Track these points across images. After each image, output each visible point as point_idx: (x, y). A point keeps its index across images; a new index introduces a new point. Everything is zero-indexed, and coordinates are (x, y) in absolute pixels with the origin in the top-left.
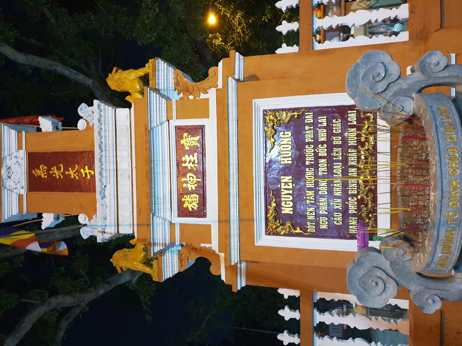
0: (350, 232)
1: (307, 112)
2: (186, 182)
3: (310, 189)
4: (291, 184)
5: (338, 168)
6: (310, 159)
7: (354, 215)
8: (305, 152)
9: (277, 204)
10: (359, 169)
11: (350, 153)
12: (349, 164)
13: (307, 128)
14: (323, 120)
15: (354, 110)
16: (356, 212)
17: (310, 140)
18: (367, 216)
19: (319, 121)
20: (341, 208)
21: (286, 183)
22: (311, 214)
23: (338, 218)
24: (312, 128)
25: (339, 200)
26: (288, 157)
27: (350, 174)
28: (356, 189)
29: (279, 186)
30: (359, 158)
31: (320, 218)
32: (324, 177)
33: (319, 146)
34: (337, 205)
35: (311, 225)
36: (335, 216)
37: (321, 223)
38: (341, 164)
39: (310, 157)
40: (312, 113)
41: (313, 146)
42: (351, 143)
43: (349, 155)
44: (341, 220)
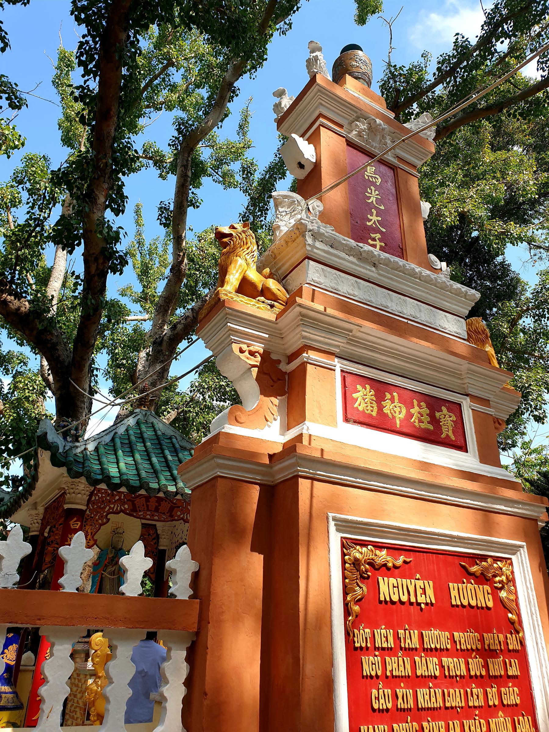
2: (392, 400)
29: (418, 576)
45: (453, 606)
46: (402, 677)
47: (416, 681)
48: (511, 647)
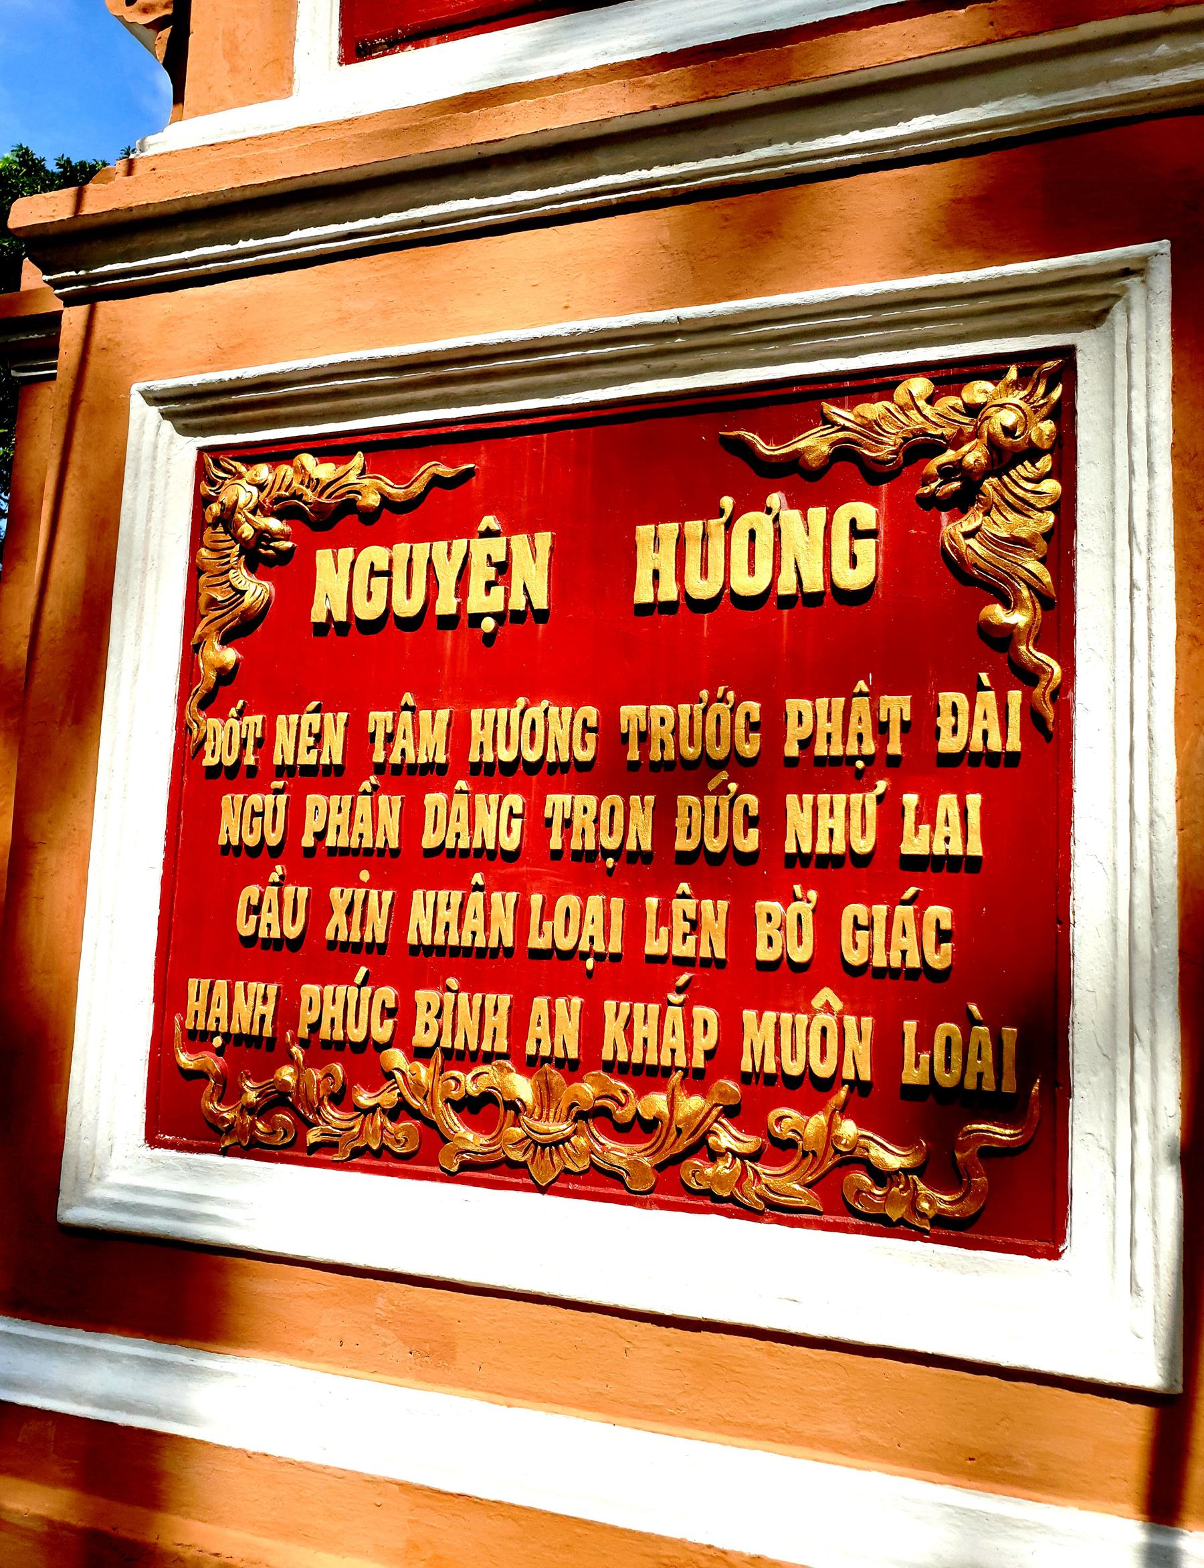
0: (193, 983)
1: (1026, 698)
3: (459, 733)
4: (495, 601)
5: (586, 923)
6: (660, 732)
7: (287, 1011)
8: (713, 699)
10: (572, 1069)
12: (609, 1006)
13: (897, 707)
14: (951, 827)
15: (1024, 1082)
16: (303, 1032)
17: (795, 733)
18: (277, 1099)
19: (947, 803)
20: (330, 934)
21: (503, 569)
23: (271, 910)
24: (895, 748)
25: (378, 930)
26: (680, 576)
27: (540, 1004)
28: (446, 1042)
30: (648, 1076)
31: (282, 798)
32: (536, 824)
33: (752, 800)
34: (349, 911)
35: (244, 743)
37: (256, 799)
38: (616, 946)
39: (675, 731)
40: (1014, 744)
41: (750, 749)
43: (675, 1015)
44: (263, 933)
45: (644, 609)
46: (356, 852)
47: (410, 866)
48: (948, 744)
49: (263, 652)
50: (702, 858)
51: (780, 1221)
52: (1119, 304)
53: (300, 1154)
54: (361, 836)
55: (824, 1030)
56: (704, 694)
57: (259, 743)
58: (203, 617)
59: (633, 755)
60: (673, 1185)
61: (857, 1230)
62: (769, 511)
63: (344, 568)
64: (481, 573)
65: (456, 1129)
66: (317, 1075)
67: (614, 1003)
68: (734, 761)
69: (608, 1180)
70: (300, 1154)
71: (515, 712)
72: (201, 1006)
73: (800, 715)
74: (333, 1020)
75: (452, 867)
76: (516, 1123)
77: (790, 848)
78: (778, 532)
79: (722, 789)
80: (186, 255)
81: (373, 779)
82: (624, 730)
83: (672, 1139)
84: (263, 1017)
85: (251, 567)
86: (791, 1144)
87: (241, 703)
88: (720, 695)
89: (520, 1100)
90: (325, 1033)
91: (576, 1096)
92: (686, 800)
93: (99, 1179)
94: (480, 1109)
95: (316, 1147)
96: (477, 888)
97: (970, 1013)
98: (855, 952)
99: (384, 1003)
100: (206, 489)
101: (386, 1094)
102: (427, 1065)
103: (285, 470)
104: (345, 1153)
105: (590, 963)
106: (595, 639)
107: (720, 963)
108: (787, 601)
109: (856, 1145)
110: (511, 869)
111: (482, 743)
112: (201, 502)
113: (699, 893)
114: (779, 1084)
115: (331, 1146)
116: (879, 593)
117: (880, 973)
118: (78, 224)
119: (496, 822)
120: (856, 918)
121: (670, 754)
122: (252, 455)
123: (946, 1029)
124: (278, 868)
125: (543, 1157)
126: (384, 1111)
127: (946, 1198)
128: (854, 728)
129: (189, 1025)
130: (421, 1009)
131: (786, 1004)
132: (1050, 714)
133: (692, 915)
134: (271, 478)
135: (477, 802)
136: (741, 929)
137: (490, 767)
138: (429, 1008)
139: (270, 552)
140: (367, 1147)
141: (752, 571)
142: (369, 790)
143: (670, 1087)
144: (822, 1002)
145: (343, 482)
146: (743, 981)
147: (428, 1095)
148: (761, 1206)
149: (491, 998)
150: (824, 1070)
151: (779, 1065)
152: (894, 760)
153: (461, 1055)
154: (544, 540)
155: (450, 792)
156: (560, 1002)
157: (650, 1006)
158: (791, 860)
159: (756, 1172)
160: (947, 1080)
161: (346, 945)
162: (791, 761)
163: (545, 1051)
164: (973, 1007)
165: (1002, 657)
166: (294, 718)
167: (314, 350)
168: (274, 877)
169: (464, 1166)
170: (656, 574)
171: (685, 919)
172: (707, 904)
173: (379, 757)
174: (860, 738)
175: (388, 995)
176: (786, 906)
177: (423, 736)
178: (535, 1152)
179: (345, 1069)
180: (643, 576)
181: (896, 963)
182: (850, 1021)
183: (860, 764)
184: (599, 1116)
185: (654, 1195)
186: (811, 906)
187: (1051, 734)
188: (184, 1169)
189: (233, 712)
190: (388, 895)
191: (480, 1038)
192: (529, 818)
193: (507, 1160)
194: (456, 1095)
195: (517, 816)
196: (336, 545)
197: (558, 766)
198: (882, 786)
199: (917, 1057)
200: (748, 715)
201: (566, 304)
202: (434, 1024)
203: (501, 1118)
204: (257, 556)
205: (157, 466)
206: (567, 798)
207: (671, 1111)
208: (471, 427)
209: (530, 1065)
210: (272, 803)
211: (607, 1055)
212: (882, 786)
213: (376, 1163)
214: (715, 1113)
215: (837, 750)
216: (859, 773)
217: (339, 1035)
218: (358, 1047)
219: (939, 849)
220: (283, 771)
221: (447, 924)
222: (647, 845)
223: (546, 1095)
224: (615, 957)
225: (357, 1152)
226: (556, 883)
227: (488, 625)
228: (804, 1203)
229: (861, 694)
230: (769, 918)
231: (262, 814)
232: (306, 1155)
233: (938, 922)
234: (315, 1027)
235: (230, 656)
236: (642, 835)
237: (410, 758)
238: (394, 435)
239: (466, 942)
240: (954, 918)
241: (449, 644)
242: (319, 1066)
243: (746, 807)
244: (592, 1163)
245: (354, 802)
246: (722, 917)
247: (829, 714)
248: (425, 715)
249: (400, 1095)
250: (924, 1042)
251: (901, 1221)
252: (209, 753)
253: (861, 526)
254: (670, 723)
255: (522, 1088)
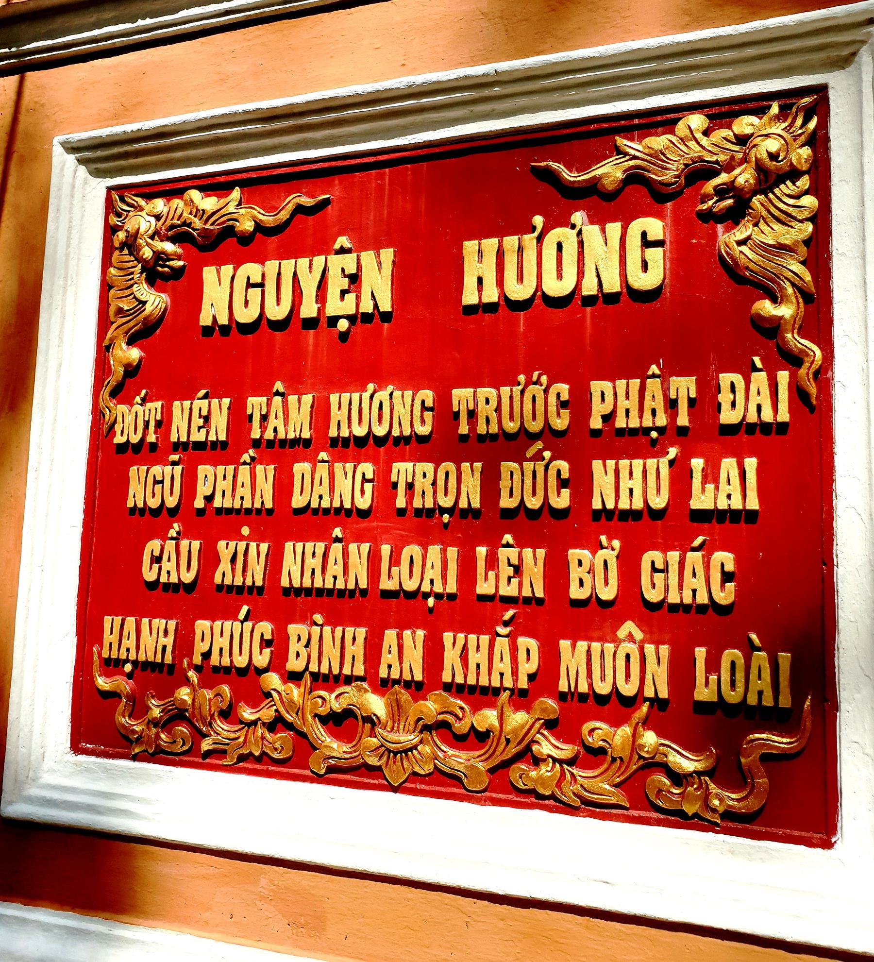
0: (108, 620)
3: (320, 414)
4: (348, 306)
5: (427, 568)
6: (484, 410)
7: (184, 642)
9: (252, 234)
10: (417, 689)
11: (514, 649)
12: (448, 637)
13: (684, 386)
14: (732, 486)
16: (197, 660)
17: (599, 409)
18: (177, 715)
19: (729, 465)
20: (218, 579)
21: (355, 279)
22: (198, 422)
23: (170, 560)
24: (683, 420)
25: (257, 575)
26: (500, 282)
27: (390, 635)
28: (313, 668)
29: (343, 241)
30: (481, 695)
31: (178, 469)
32: (385, 487)
33: (563, 466)
34: (233, 560)
35: (147, 424)
36: (184, 543)
37: (157, 470)
38: (452, 587)
39: (498, 409)
40: (784, 415)
41: (561, 423)
42: (573, 656)
43: (502, 644)
45: (471, 310)
46: (238, 511)
47: (282, 522)
48: (728, 417)
49: (163, 351)
50: (522, 513)
51: (593, 815)
52: (865, 47)
53: (196, 760)
54: (242, 498)
55: (628, 656)
56: (522, 378)
57: (158, 424)
58: (113, 323)
59: (464, 429)
60: (504, 785)
61: (658, 823)
62: (573, 227)
63: (226, 282)
64: (337, 283)
65: (323, 739)
66: (209, 694)
67: (452, 634)
68: (548, 433)
69: (449, 781)
70: (196, 760)
71: (366, 396)
72: (114, 638)
73: (603, 394)
74: (221, 649)
75: (316, 522)
76: (373, 734)
77: (597, 504)
78: (581, 244)
79: (538, 457)
80: (96, 32)
81: (251, 452)
82: (455, 409)
83: (501, 747)
84: (164, 648)
85: (151, 282)
86: (602, 751)
87: (144, 392)
88: (535, 378)
89: (375, 715)
90: (215, 660)
91: (422, 712)
92: (508, 466)
93: (33, 780)
94: (342, 722)
95: (208, 754)
96: (337, 540)
97: (750, 641)
98: (654, 591)
99: (262, 635)
100: (114, 220)
101: (265, 710)
102: (299, 687)
103: (177, 203)
104: (233, 758)
105: (431, 602)
106: (430, 333)
107: (540, 601)
108: (589, 301)
109: (656, 752)
110: (364, 524)
111: (339, 422)
112: (110, 230)
113: (521, 543)
114: (591, 702)
115: (221, 753)
116: (667, 291)
117: (674, 608)
118: (10, 11)
119: (350, 485)
120: (653, 563)
121: (494, 429)
122: (150, 191)
123: (732, 654)
124: (176, 525)
125: (395, 762)
126: (264, 724)
127: (734, 796)
128: (648, 404)
129: (105, 654)
130: (293, 639)
131: (596, 634)
132: (813, 390)
133: (515, 561)
134: (166, 210)
135: (335, 470)
136: (557, 572)
137: (346, 441)
138: (299, 639)
139: (166, 269)
140: (251, 754)
141: (560, 276)
142: (248, 461)
143: (499, 704)
144: (626, 633)
145: (223, 212)
146: (557, 616)
147: (299, 711)
148: (577, 803)
149: (350, 631)
150: (628, 689)
151: (591, 686)
152: (682, 431)
153: (326, 677)
154: (388, 255)
155: (314, 462)
156: (407, 634)
157: (481, 637)
158: (597, 515)
159: (572, 774)
160: (733, 697)
161: (231, 588)
162: (596, 433)
163: (395, 675)
164: (754, 636)
165: (772, 343)
166: (187, 403)
167: (199, 106)
168: (172, 533)
169: (331, 769)
170: (480, 280)
171: (510, 565)
172: (528, 552)
173: (256, 434)
174: (654, 412)
175: (266, 628)
176: (594, 553)
177: (292, 417)
178: (388, 758)
179: (232, 690)
180: (470, 282)
181: (688, 600)
182: (650, 648)
183: (654, 434)
184: (441, 728)
185: (487, 794)
186: (615, 553)
187: (814, 408)
188: (102, 772)
189: (138, 399)
190: (264, 547)
191: (342, 664)
192: (378, 482)
193: (365, 765)
194: (323, 711)
195: (368, 481)
196: (219, 262)
197: (402, 440)
198: (673, 452)
199: (707, 679)
200: (558, 395)
201: (403, 62)
202: (304, 653)
203: (360, 729)
204: (155, 273)
205: (74, 202)
206: (409, 465)
207: (501, 725)
208: (327, 164)
209: (383, 686)
210: (170, 472)
211: (447, 677)
212: (673, 452)
213: (258, 767)
214: (537, 725)
215: (634, 423)
216: (654, 442)
217: (226, 662)
218: (242, 672)
219: (722, 504)
220: (178, 446)
221: (313, 570)
222: (476, 504)
223: (397, 711)
224: (451, 597)
225: (242, 758)
226: (402, 536)
227: (343, 325)
228: (613, 800)
229: (654, 376)
230: (580, 563)
231: (161, 482)
232: (201, 760)
233: (722, 565)
234: (207, 655)
235: (135, 354)
236: (471, 493)
237: (281, 435)
238: (265, 173)
239: (329, 585)
240: (737, 562)
241: (311, 341)
242: (211, 688)
243: (559, 471)
244: (436, 767)
245: (236, 471)
246: (541, 563)
247: (627, 393)
248: (292, 399)
249: (277, 711)
250: (713, 665)
251: (696, 815)
252: (119, 433)
253: (650, 238)
254: (494, 403)
255: (376, 705)
